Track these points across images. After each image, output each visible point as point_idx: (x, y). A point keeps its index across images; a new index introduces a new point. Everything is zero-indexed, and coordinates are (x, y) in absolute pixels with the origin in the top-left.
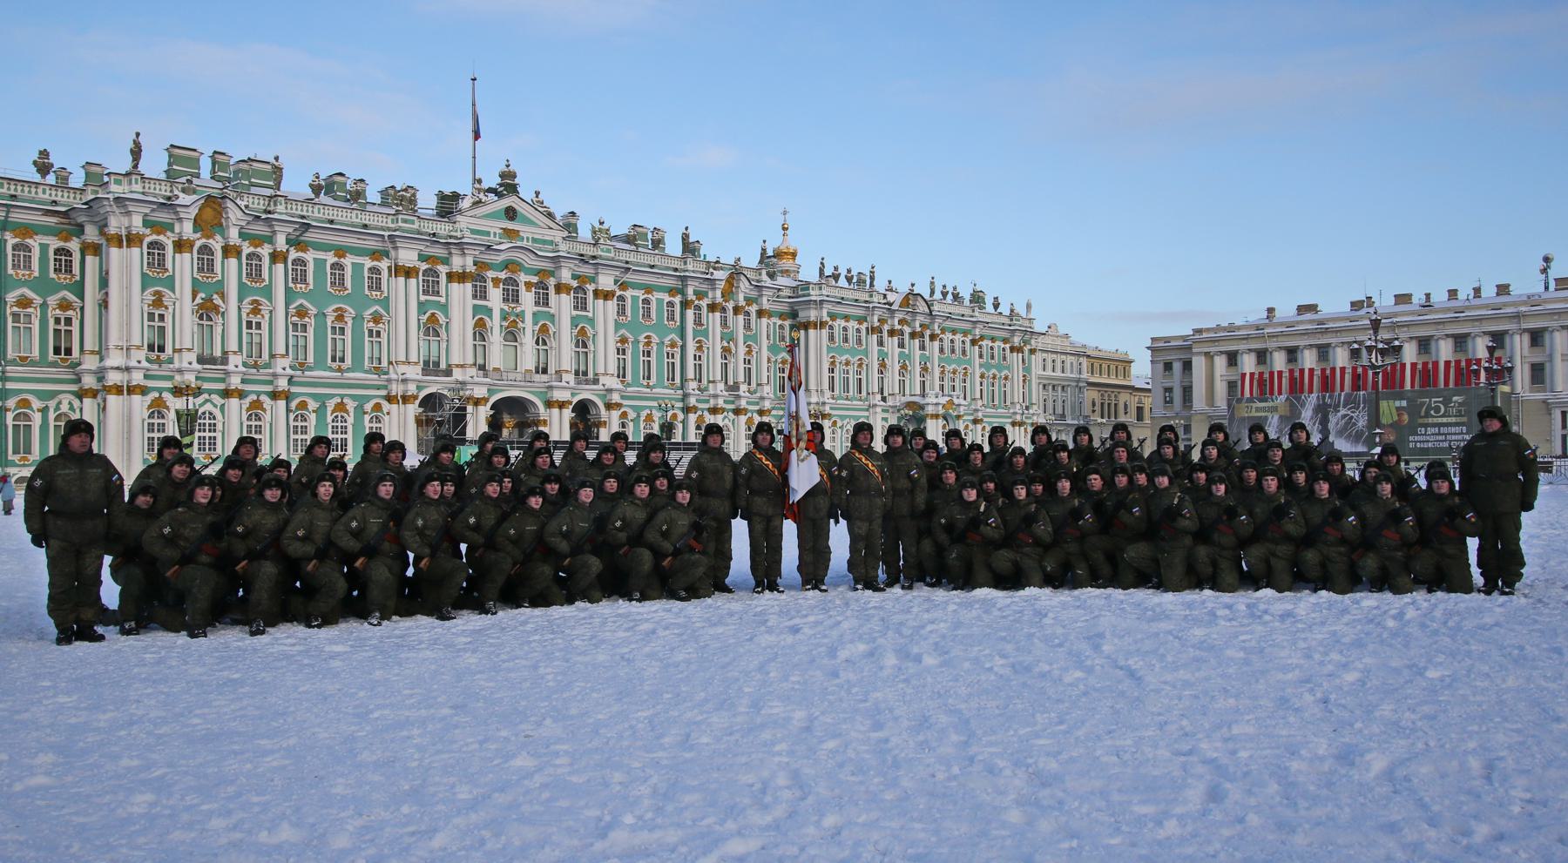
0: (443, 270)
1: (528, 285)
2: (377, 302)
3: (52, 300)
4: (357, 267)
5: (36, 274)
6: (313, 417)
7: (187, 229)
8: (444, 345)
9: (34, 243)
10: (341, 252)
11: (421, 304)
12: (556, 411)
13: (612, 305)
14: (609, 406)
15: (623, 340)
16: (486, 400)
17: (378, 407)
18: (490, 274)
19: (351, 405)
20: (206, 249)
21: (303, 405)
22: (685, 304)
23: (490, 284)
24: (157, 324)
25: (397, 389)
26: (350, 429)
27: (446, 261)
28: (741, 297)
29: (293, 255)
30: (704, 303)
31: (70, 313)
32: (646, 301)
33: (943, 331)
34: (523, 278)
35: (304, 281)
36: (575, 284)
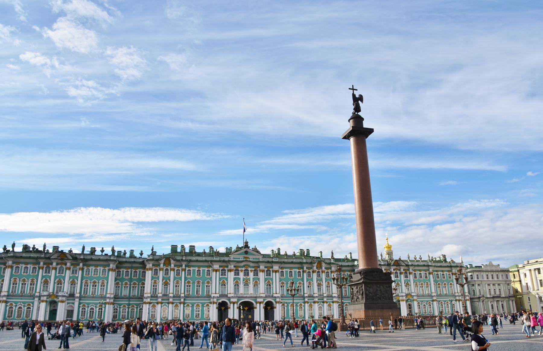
0: (226, 269)
2: (209, 278)
4: (204, 271)
6: (191, 308)
7: (162, 265)
9: (138, 271)
10: (199, 267)
12: (258, 305)
14: (276, 302)
15: (283, 283)
16: (237, 303)
17: (208, 305)
18: (240, 269)
19: (200, 305)
20: (167, 270)
22: (304, 272)
25: (212, 300)
27: (227, 267)
28: (323, 268)
29: (187, 269)
30: (311, 271)
32: (291, 272)
33: (415, 270)
34: (249, 269)
35: (190, 275)
36: (266, 269)
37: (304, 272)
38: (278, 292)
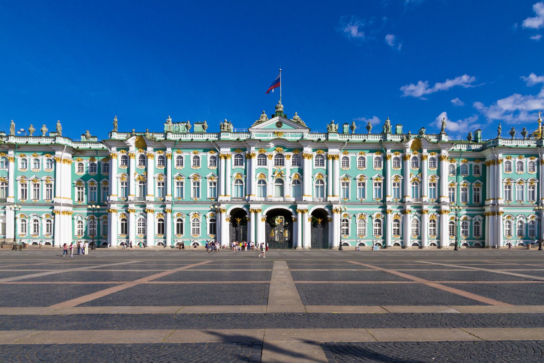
11: (232, 169)
26: (200, 224)
34: (286, 154)
38: (337, 193)
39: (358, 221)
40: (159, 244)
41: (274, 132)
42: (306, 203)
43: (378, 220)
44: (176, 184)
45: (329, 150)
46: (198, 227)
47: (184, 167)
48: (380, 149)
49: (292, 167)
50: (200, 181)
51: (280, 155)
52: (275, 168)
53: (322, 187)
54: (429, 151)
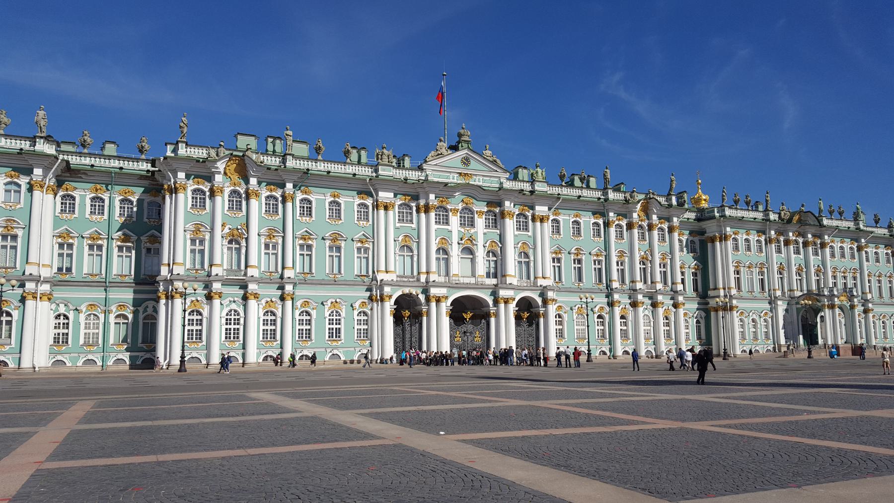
1: (480, 213)
3: (144, 238)
5: (134, 219)
8: (415, 259)
12: (502, 306)
13: (548, 226)
14: (545, 302)
16: (447, 298)
21: (306, 303)
22: (607, 225)
23: (450, 214)
24: (198, 247)
26: (343, 320)
28: (655, 217)
29: (299, 196)
31: (156, 245)
37: (607, 225)
39: (575, 317)
40: (265, 359)
41: (460, 174)
42: (511, 287)
43: (600, 317)
44: (298, 248)
45: (538, 208)
46: (338, 326)
47: (313, 219)
48: (600, 210)
49: (486, 231)
50: (343, 244)
51: (468, 210)
52: (463, 230)
53: (528, 264)
54: (660, 218)
